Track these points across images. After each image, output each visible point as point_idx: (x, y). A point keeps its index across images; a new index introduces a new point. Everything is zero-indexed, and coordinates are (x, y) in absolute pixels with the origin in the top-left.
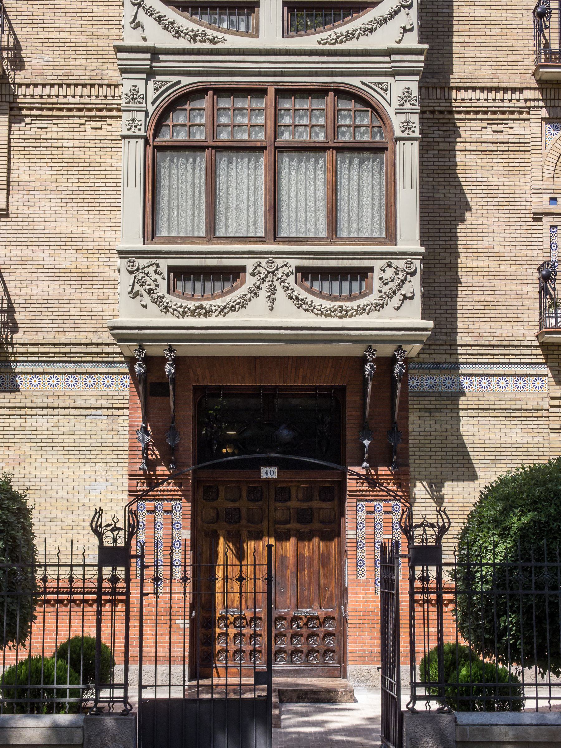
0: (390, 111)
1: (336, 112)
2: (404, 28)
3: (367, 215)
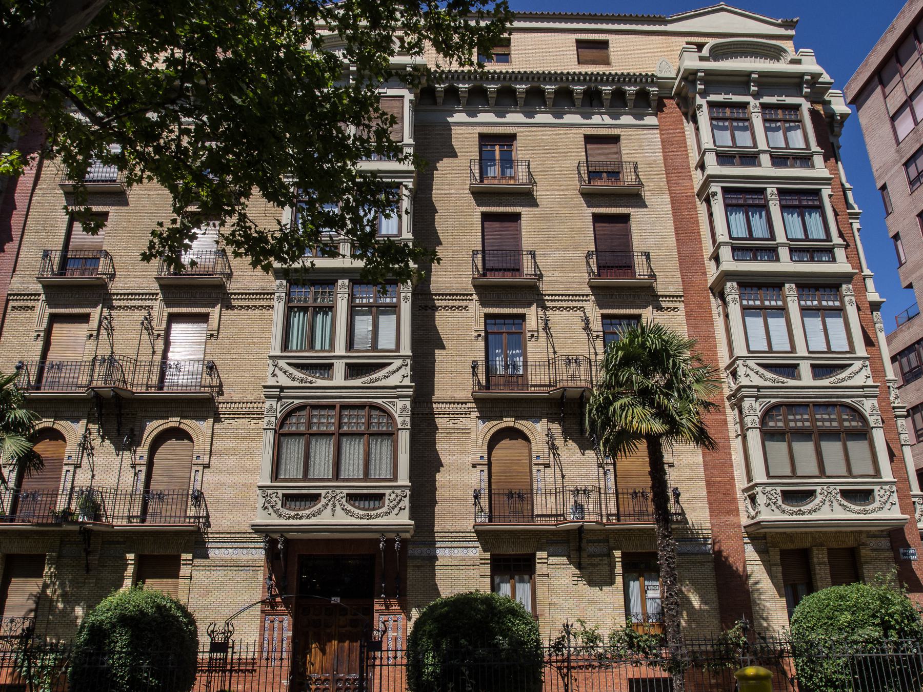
0: (396, 416)
1: (370, 416)
3: (384, 466)
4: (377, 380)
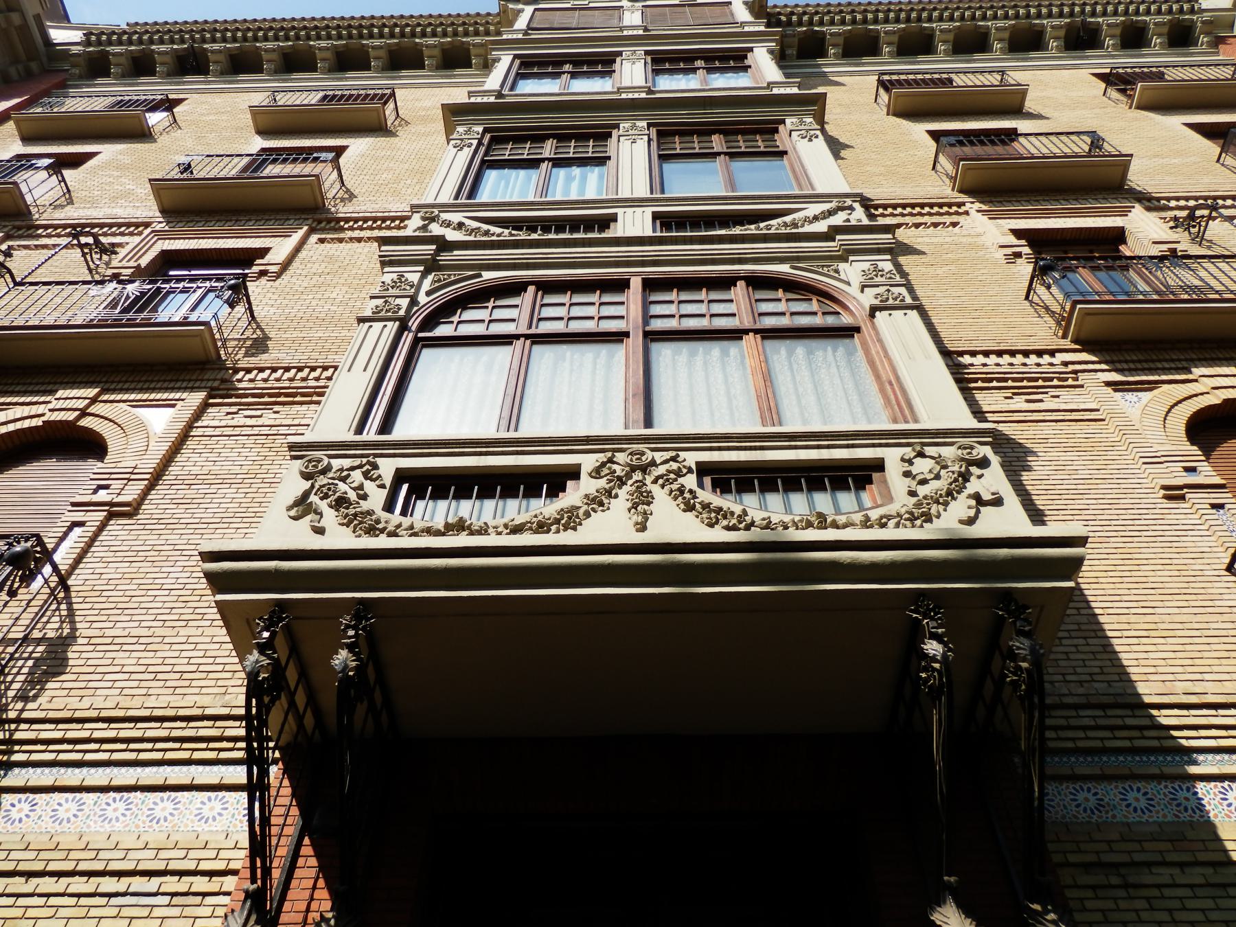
0: (854, 290)
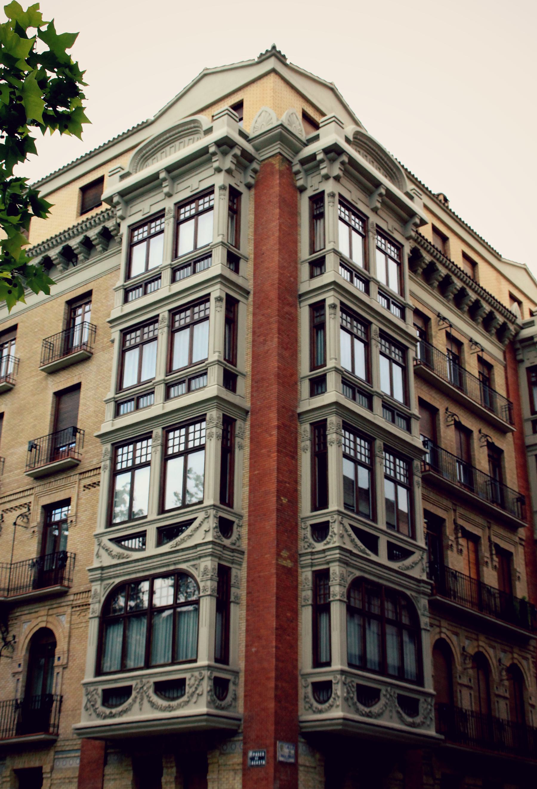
2: (206, 531)
4: (183, 541)
